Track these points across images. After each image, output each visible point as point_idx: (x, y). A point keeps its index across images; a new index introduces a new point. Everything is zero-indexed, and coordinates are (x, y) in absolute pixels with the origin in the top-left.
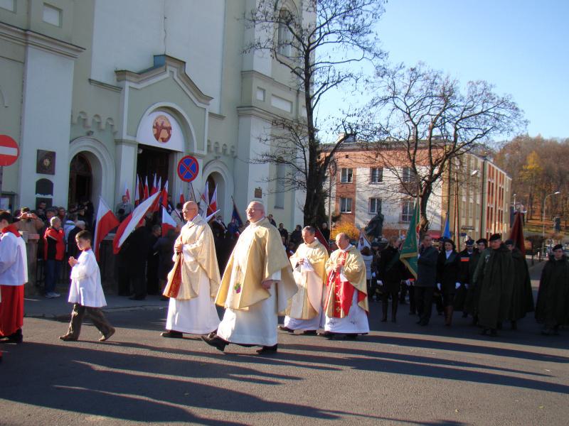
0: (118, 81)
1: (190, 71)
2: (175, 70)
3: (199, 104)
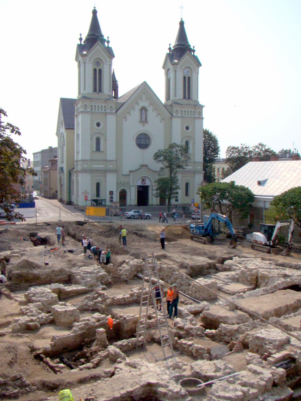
0: (130, 173)
1: (149, 167)
2: (145, 168)
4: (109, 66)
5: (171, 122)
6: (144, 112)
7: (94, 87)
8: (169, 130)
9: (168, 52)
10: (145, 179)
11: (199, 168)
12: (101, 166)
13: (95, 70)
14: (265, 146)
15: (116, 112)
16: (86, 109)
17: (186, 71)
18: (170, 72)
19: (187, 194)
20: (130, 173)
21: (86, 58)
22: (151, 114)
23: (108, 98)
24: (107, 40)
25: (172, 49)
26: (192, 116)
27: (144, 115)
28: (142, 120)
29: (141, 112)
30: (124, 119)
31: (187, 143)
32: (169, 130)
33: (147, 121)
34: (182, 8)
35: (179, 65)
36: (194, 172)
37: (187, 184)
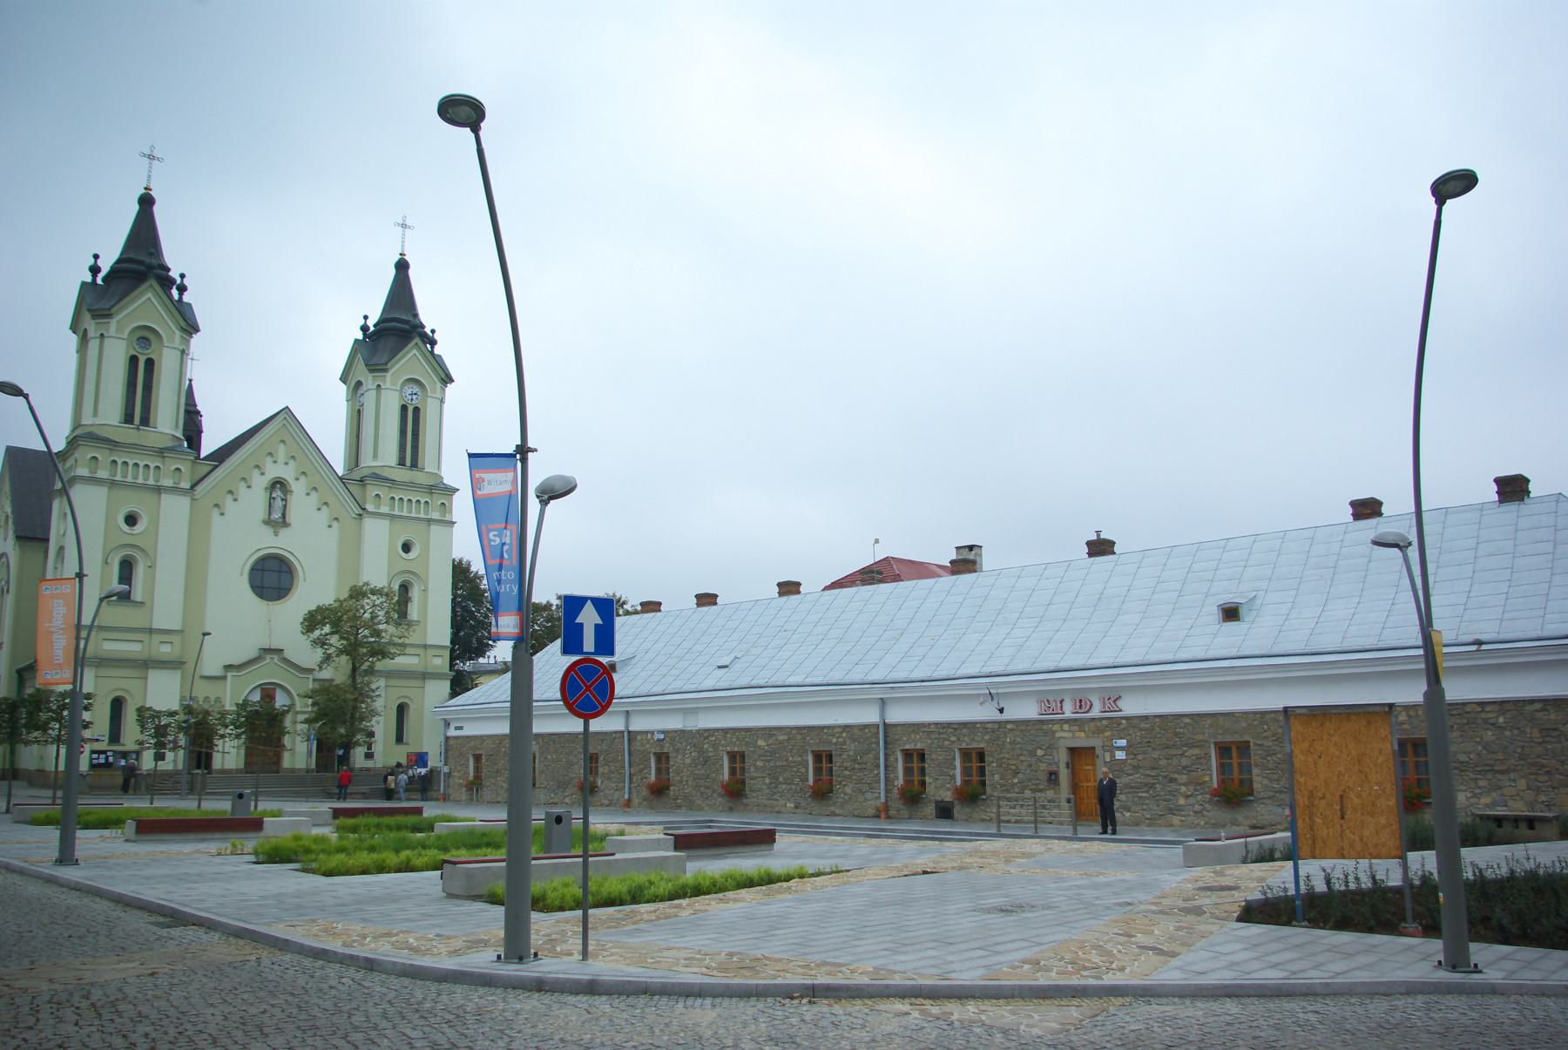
1: (288, 654)
2: (276, 658)
3: (301, 676)
4: (179, 353)
5: (360, 527)
6: (278, 493)
7: (126, 409)
8: (351, 552)
9: (360, 336)
10: (274, 689)
11: (438, 661)
12: (132, 648)
13: (133, 360)
14: (624, 603)
15: (193, 487)
16: (96, 473)
17: (409, 391)
18: (364, 388)
19: (400, 739)
20: (226, 672)
21: (109, 323)
22: (301, 504)
23: (169, 444)
24: (179, 281)
25: (372, 329)
26: (422, 515)
27: (279, 503)
28: (272, 517)
29: (271, 494)
30: (216, 512)
31: (405, 588)
32: (351, 552)
33: (287, 520)
34: (404, 226)
35: (391, 372)
36: (424, 676)
37: (402, 710)
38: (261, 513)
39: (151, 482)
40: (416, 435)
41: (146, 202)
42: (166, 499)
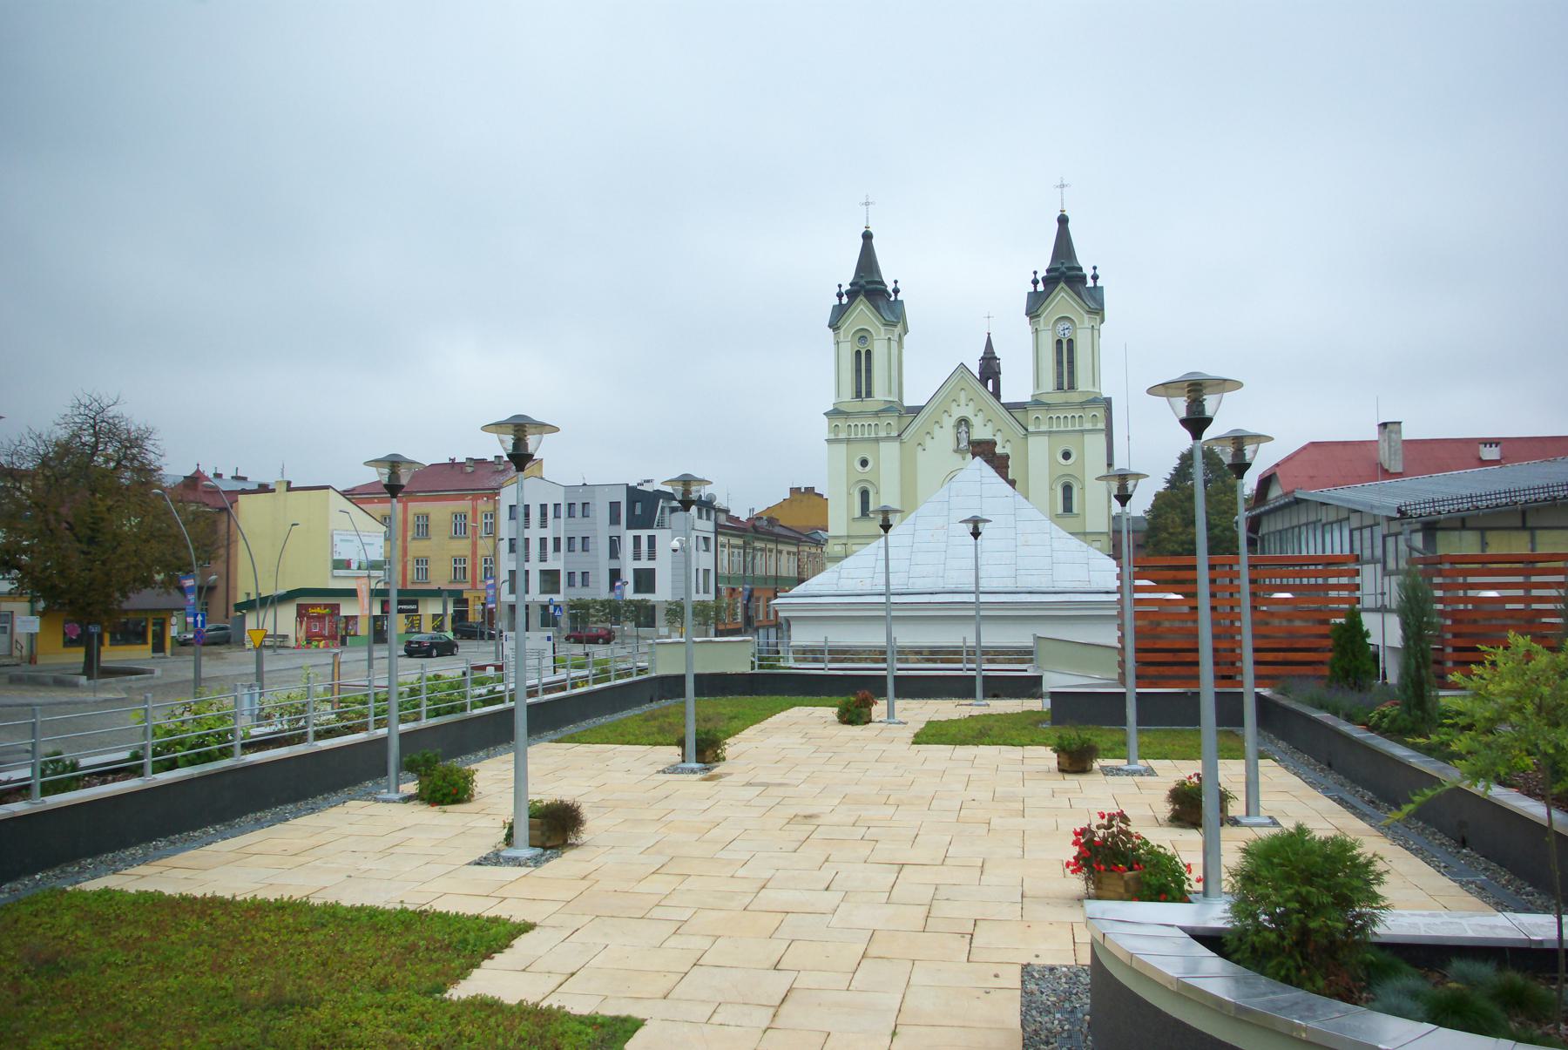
6: (963, 428)
23: (883, 407)
26: (1077, 428)
29: (958, 429)
38: (952, 444)
39: (873, 435)
40: (1071, 362)
41: (867, 237)
42: (881, 444)
